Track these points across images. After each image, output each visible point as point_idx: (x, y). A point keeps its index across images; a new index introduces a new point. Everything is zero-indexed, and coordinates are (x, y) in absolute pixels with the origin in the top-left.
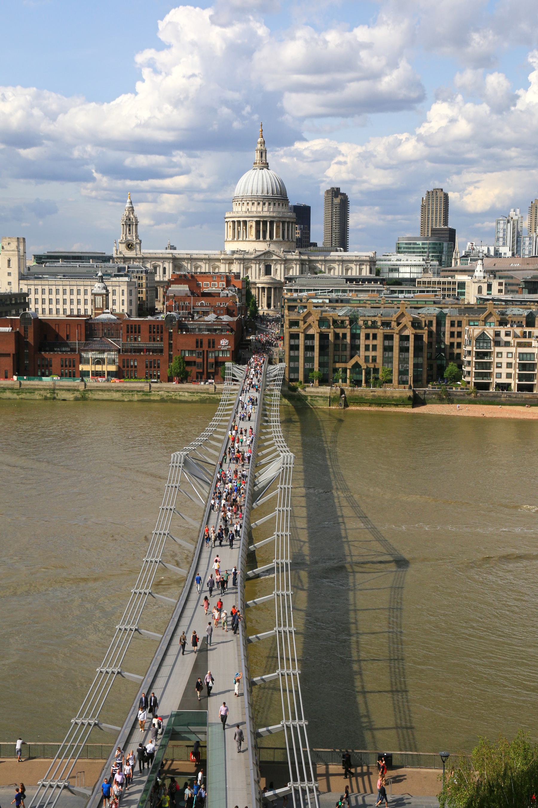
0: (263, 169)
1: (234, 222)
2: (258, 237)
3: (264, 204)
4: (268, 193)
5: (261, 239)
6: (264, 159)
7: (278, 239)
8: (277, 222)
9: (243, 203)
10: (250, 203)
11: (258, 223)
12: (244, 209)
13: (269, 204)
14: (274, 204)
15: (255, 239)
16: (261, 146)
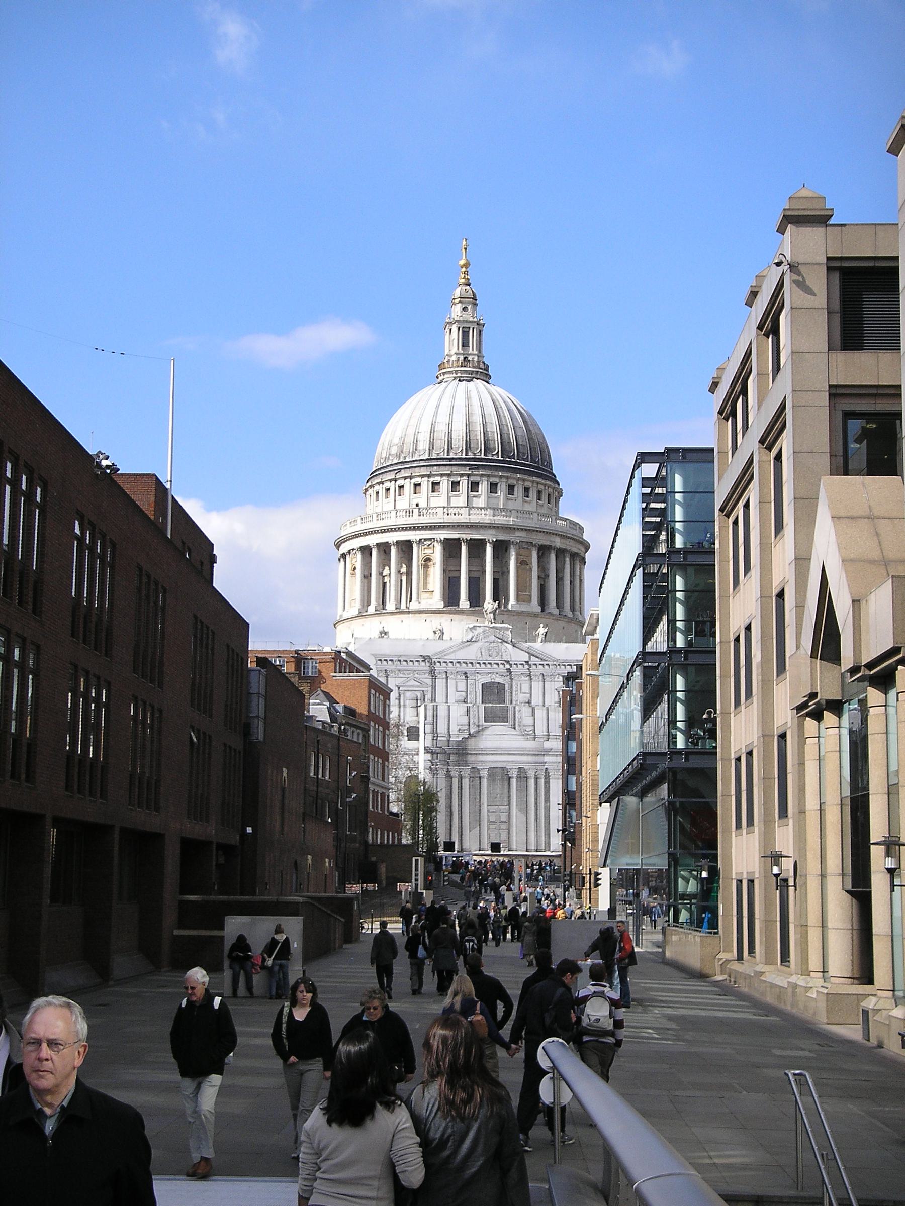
0: (469, 381)
1: (366, 551)
2: (451, 597)
3: (474, 486)
4: (487, 450)
5: (464, 603)
6: (472, 350)
7: (524, 608)
8: (525, 546)
9: (401, 487)
10: (425, 484)
11: (451, 548)
12: (403, 503)
13: (493, 488)
14: (511, 489)
15: (440, 605)
16: (465, 309)
